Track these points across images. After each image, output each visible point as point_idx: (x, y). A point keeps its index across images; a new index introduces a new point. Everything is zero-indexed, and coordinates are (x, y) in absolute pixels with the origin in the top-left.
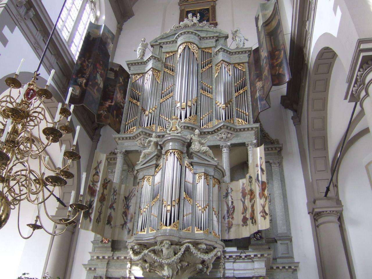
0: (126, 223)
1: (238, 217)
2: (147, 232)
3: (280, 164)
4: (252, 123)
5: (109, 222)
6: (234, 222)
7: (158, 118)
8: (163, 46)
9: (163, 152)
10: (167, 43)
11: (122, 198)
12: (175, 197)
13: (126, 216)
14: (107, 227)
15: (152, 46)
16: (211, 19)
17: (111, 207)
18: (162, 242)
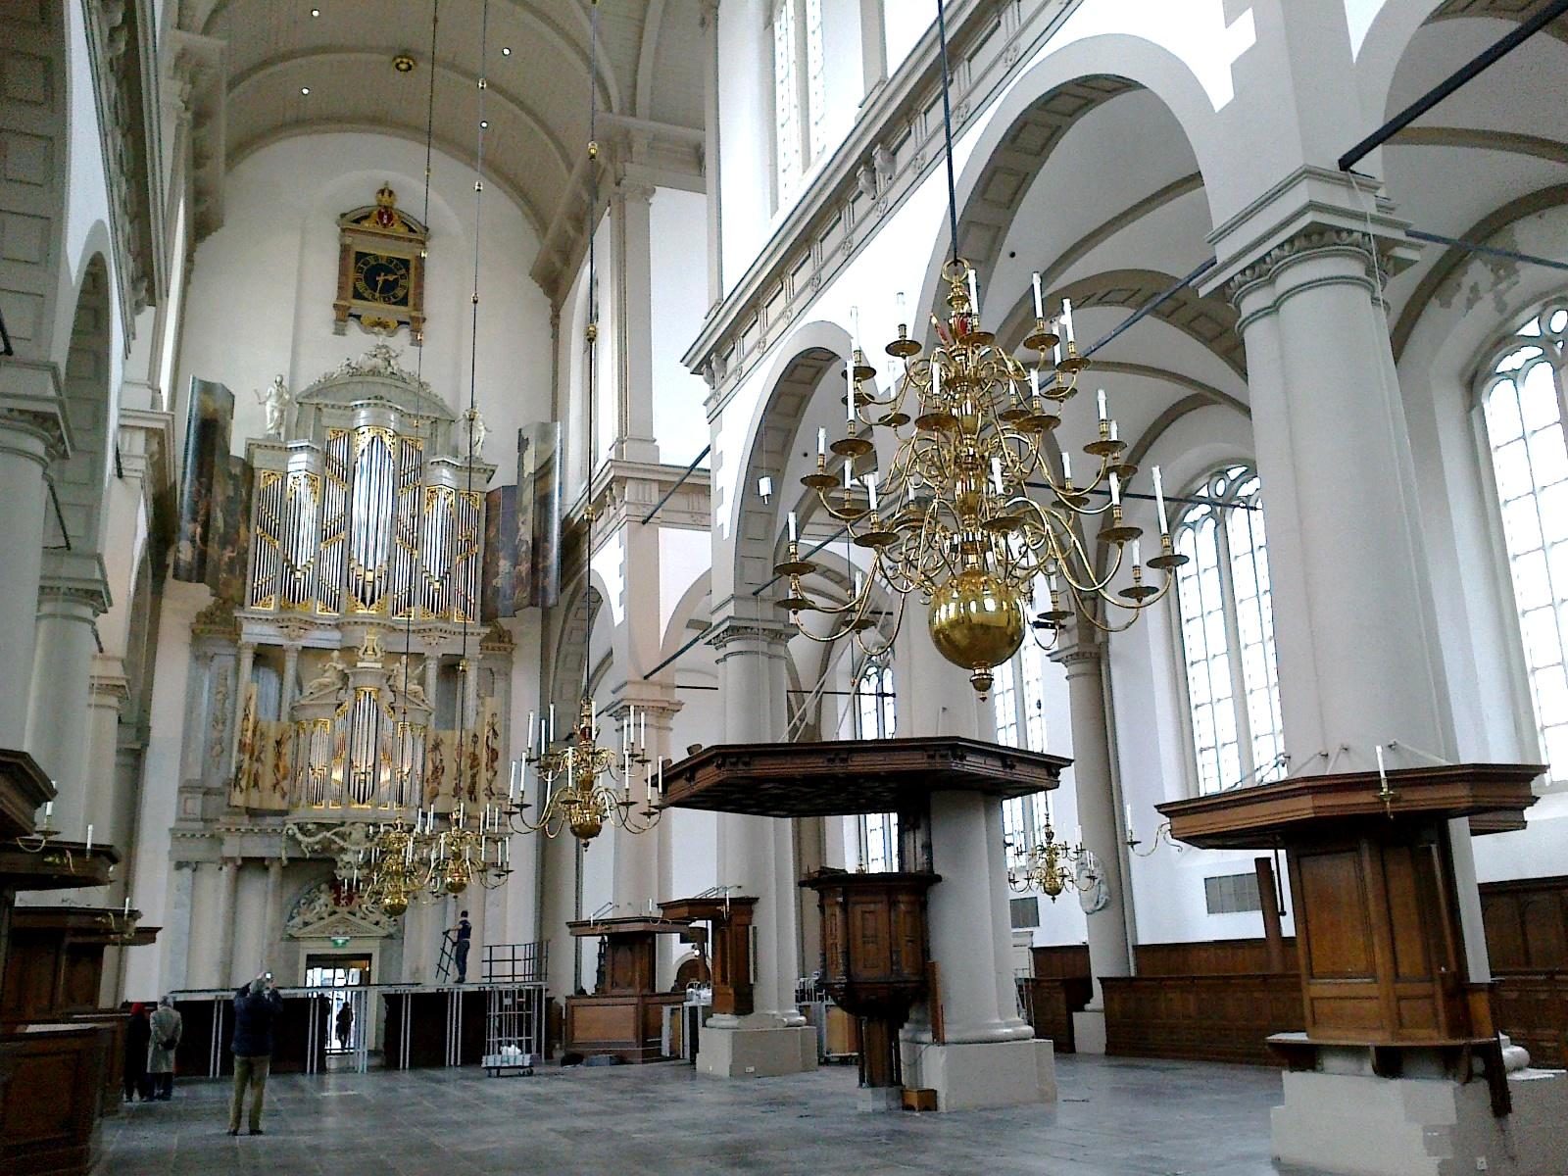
0: (278, 783)
1: (447, 784)
2: (327, 806)
3: (507, 675)
4: (478, 618)
5: (256, 784)
6: (442, 790)
7: (316, 583)
8: (325, 410)
9: (350, 685)
10: (333, 407)
11: (271, 743)
12: (370, 763)
13: (279, 771)
14: (254, 793)
15: (300, 404)
16: (411, 302)
17: (259, 760)
18: (353, 824)
